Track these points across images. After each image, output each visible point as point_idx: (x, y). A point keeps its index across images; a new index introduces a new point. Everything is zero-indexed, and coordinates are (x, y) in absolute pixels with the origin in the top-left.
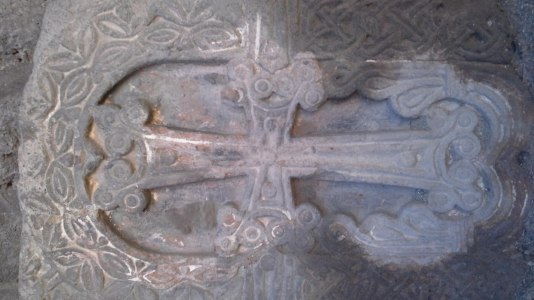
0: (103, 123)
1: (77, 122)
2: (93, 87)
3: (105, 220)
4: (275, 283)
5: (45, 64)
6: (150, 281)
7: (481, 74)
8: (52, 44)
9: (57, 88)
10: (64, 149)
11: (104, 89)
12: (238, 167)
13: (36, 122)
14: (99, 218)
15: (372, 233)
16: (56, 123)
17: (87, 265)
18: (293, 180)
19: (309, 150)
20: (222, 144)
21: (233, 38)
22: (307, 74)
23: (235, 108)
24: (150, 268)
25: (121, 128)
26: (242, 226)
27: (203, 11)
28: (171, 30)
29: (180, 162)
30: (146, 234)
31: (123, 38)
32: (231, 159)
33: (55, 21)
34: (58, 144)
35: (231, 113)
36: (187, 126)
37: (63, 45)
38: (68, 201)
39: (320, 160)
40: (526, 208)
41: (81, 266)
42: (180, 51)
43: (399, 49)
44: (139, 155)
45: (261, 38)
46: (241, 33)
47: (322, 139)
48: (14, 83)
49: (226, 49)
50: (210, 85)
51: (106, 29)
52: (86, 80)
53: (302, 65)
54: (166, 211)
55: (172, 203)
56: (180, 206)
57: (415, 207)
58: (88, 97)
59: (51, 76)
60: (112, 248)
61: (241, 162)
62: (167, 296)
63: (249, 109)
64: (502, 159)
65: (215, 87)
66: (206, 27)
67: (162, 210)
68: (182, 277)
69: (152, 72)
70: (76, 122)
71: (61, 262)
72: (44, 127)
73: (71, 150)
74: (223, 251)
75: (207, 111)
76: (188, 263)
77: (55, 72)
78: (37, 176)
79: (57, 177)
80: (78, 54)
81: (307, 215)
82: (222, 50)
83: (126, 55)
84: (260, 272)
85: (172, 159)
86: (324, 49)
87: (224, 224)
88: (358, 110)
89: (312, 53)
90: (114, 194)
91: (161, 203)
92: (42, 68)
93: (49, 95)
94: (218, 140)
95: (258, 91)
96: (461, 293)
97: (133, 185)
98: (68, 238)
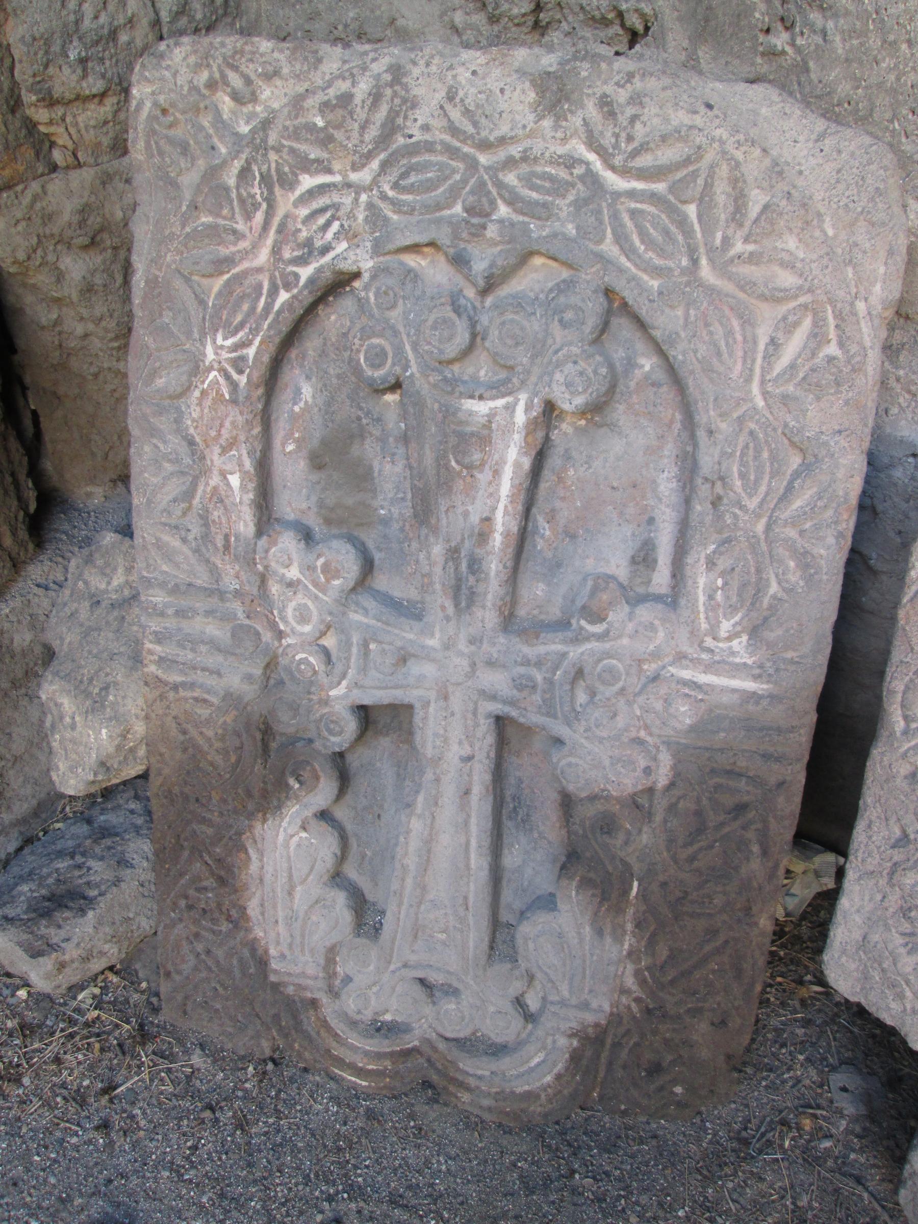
0: (562, 299)
1: (570, 229)
2: (652, 278)
3: (338, 284)
4: (207, 647)
5: (724, 153)
6: (205, 386)
7: (584, 1062)
8: (777, 170)
9: (659, 181)
10: (507, 195)
11: (643, 312)
12: (440, 601)
13: (576, 121)
14: (341, 273)
15: (304, 835)
16: (572, 174)
17: (238, 239)
19: (466, 751)
20: (493, 574)
21: (726, 626)
22: (622, 770)
23: (573, 601)
24: (234, 385)
25: (544, 345)
26: (316, 597)
27: (797, 566)
28: (763, 489)
29: (459, 474)
30: (310, 369)
31: (762, 368)
32: (457, 589)
33: (839, 171)
34: (518, 178)
35: (563, 589)
36: (543, 486)
37: (766, 207)
38: (384, 197)
39: (445, 766)
40: (343, 1079)
41: (237, 223)
42: (712, 503)
43: (652, 942)
44: (482, 373)
45: (712, 687)
46: (735, 643)
47: (488, 777)
48: (709, 8)
49: (701, 608)
50: (630, 553)
51: (788, 326)
52: (671, 264)
53: (642, 763)
54: (359, 419)
55: (377, 432)
56: (369, 450)
57: (347, 917)
58: (628, 264)
59: (691, 168)
60: (274, 301)
61: (451, 610)
62: (178, 421)
63: (564, 642)
64: (429, 1060)
65: (624, 563)
66: (758, 571)
67: (361, 409)
68: (216, 457)
69: (678, 417)
70: (570, 226)
71: (245, 173)
73: (503, 210)
74: (267, 551)
75: (573, 537)
76: (244, 475)
77: (700, 181)
78: (446, 115)
79: (439, 170)
80: (739, 247)
81: (337, 729)
82: (702, 599)
83: (720, 374)
84: (227, 617)
85: (467, 460)
86: (672, 808)
87: (321, 561)
88: (545, 838)
89: (667, 782)
90: (395, 315)
91: (377, 409)
92: (716, 145)
93: (644, 161)
94: (501, 567)
95: (601, 665)
96: (203, 957)
97: (413, 363)
98: (298, 193)
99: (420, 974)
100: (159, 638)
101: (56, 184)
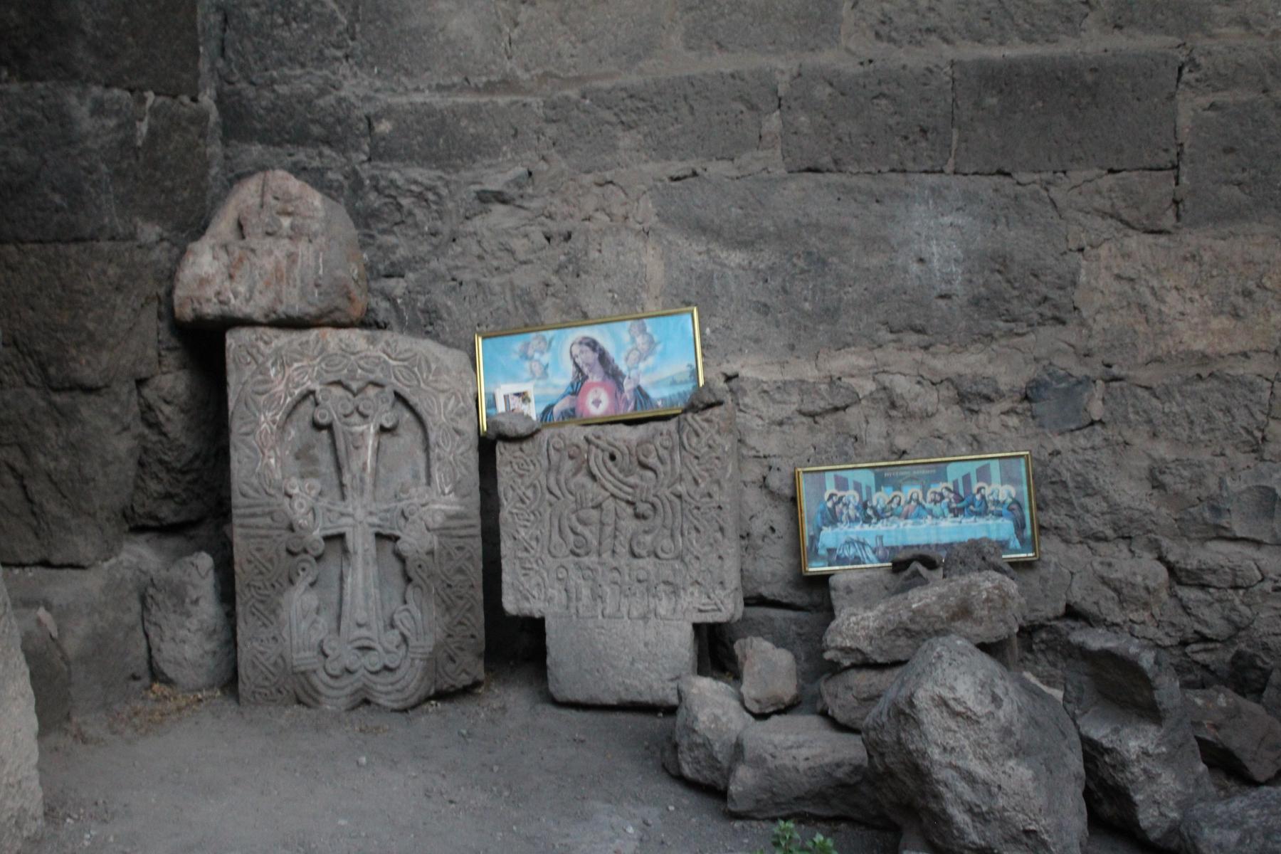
8: (437, 359)
18: (341, 537)
21: (447, 490)
51: (449, 399)
56: (316, 452)
72: (376, 351)
73: (359, 371)
80: (431, 378)
86: (440, 555)
90: (328, 403)
99: (358, 643)
100: (242, 526)
101: (163, 378)
